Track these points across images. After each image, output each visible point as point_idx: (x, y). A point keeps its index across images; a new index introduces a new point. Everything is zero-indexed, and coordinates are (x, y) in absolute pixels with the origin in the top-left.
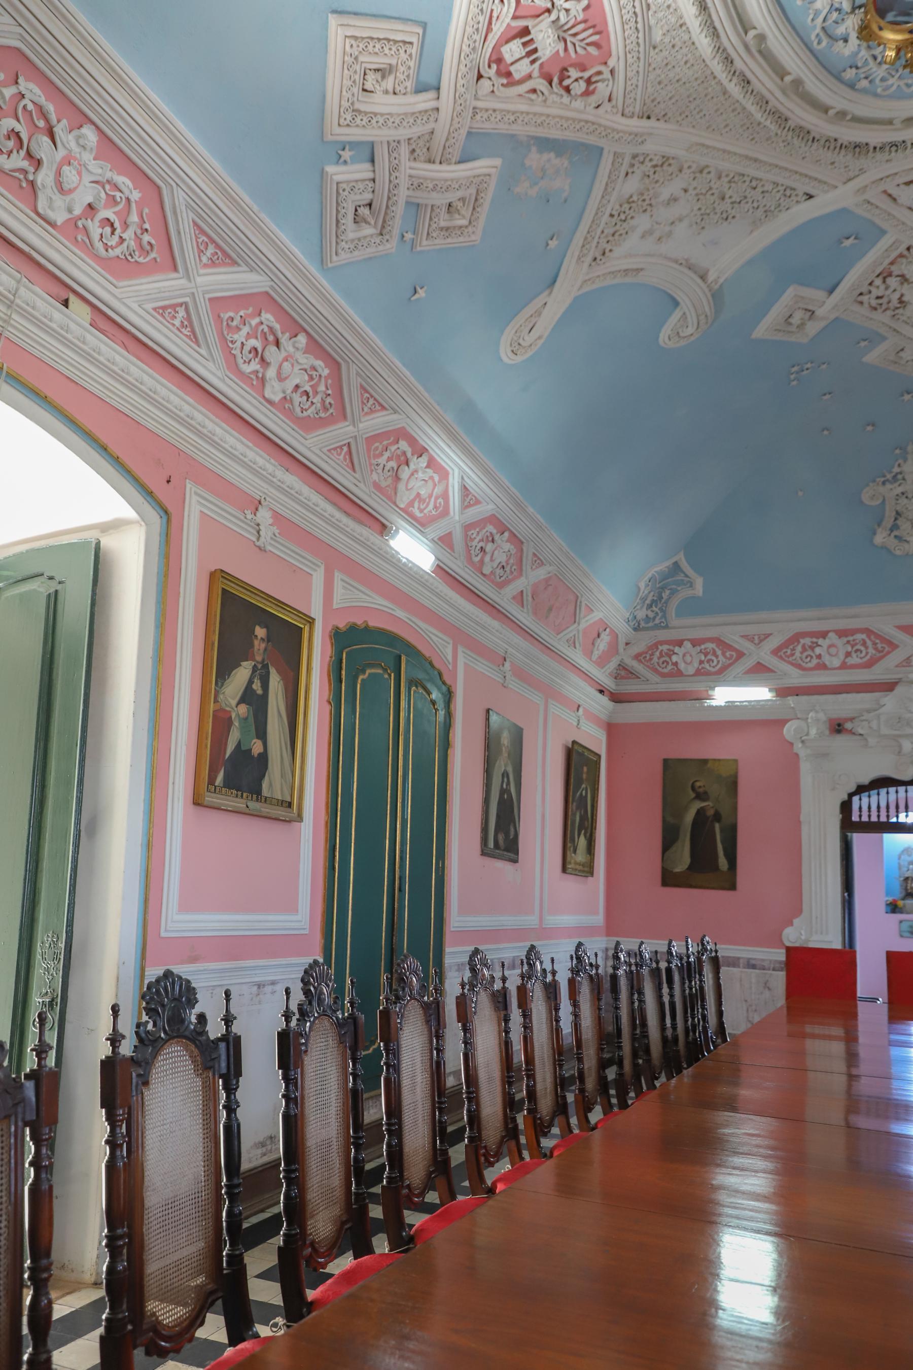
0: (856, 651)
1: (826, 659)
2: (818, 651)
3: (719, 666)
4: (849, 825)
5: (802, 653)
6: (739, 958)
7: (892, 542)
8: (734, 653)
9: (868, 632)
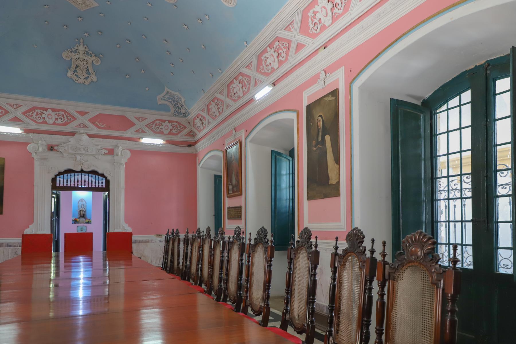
0: (60, 118)
1: (47, 120)
2: (43, 116)
4: (54, 187)
6: (3, 243)
7: (74, 77)
9: (64, 111)
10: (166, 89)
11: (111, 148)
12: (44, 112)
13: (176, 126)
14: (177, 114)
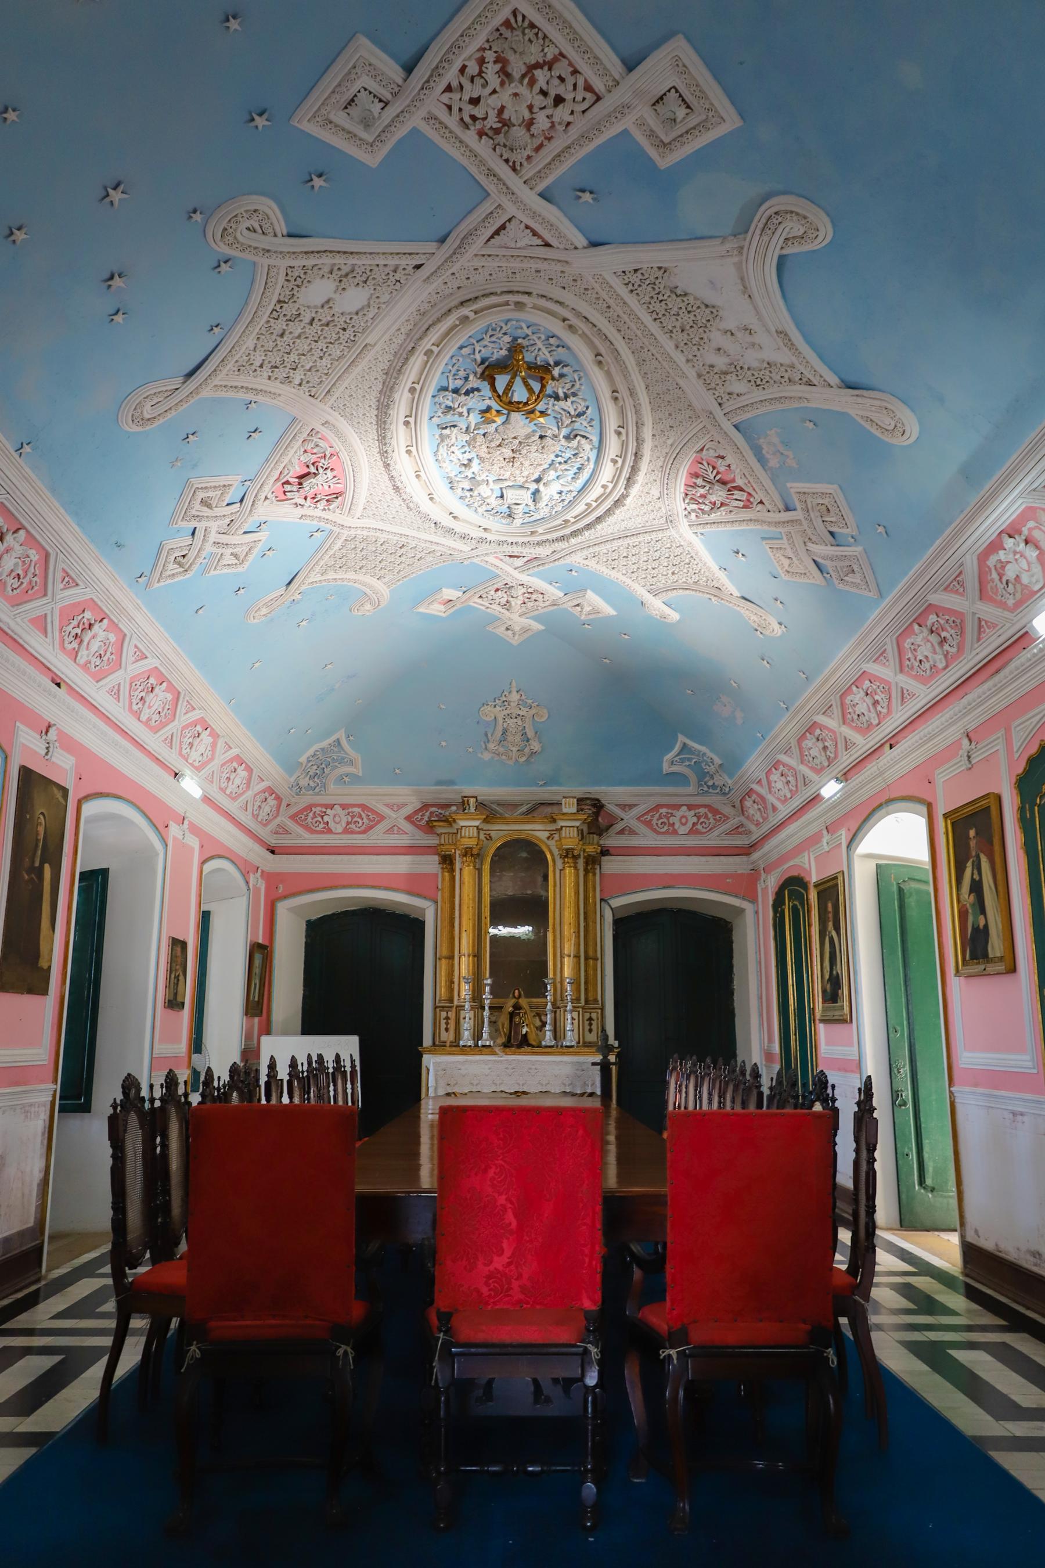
10: (681, 739)
13: (706, 817)
14: (706, 789)
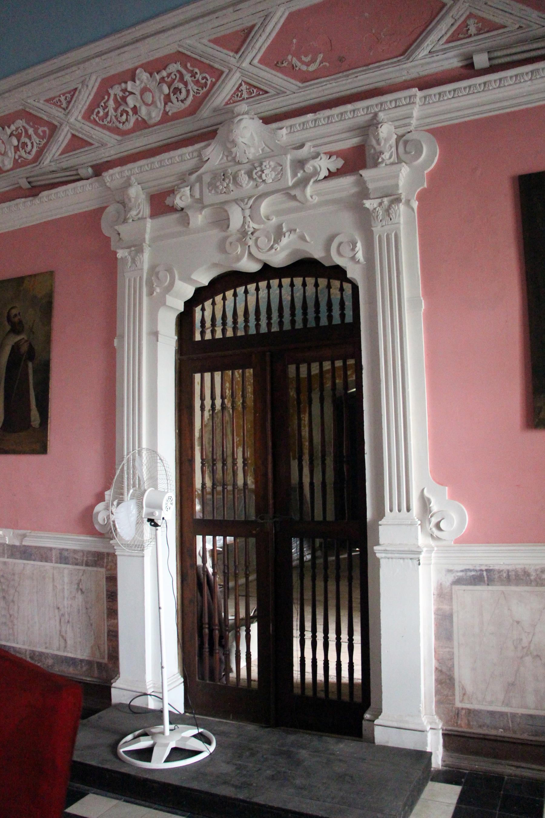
3: (35, 150)
5: (116, 110)
8: (46, 129)
9: (180, 57)
11: (354, 142)
12: (130, 86)
